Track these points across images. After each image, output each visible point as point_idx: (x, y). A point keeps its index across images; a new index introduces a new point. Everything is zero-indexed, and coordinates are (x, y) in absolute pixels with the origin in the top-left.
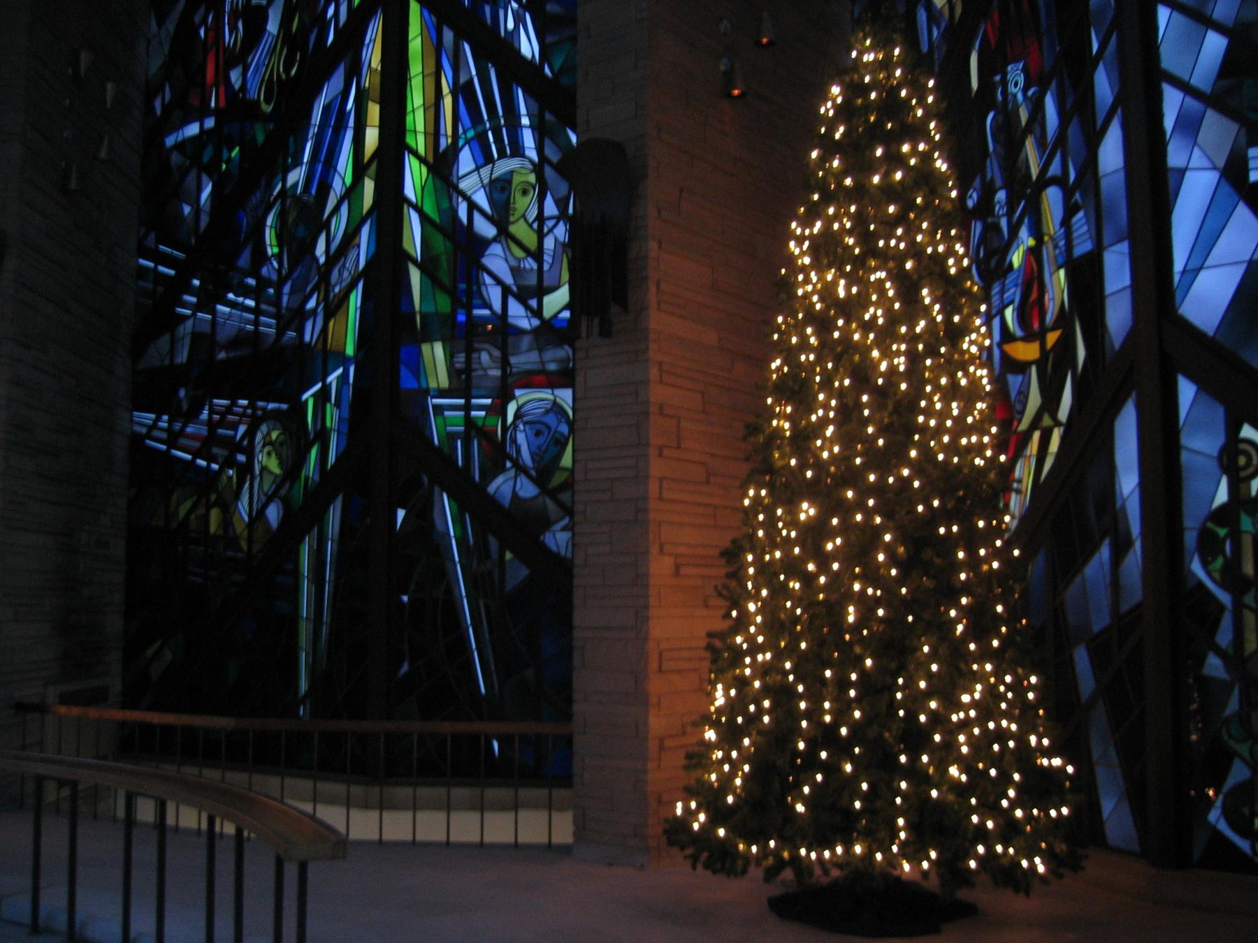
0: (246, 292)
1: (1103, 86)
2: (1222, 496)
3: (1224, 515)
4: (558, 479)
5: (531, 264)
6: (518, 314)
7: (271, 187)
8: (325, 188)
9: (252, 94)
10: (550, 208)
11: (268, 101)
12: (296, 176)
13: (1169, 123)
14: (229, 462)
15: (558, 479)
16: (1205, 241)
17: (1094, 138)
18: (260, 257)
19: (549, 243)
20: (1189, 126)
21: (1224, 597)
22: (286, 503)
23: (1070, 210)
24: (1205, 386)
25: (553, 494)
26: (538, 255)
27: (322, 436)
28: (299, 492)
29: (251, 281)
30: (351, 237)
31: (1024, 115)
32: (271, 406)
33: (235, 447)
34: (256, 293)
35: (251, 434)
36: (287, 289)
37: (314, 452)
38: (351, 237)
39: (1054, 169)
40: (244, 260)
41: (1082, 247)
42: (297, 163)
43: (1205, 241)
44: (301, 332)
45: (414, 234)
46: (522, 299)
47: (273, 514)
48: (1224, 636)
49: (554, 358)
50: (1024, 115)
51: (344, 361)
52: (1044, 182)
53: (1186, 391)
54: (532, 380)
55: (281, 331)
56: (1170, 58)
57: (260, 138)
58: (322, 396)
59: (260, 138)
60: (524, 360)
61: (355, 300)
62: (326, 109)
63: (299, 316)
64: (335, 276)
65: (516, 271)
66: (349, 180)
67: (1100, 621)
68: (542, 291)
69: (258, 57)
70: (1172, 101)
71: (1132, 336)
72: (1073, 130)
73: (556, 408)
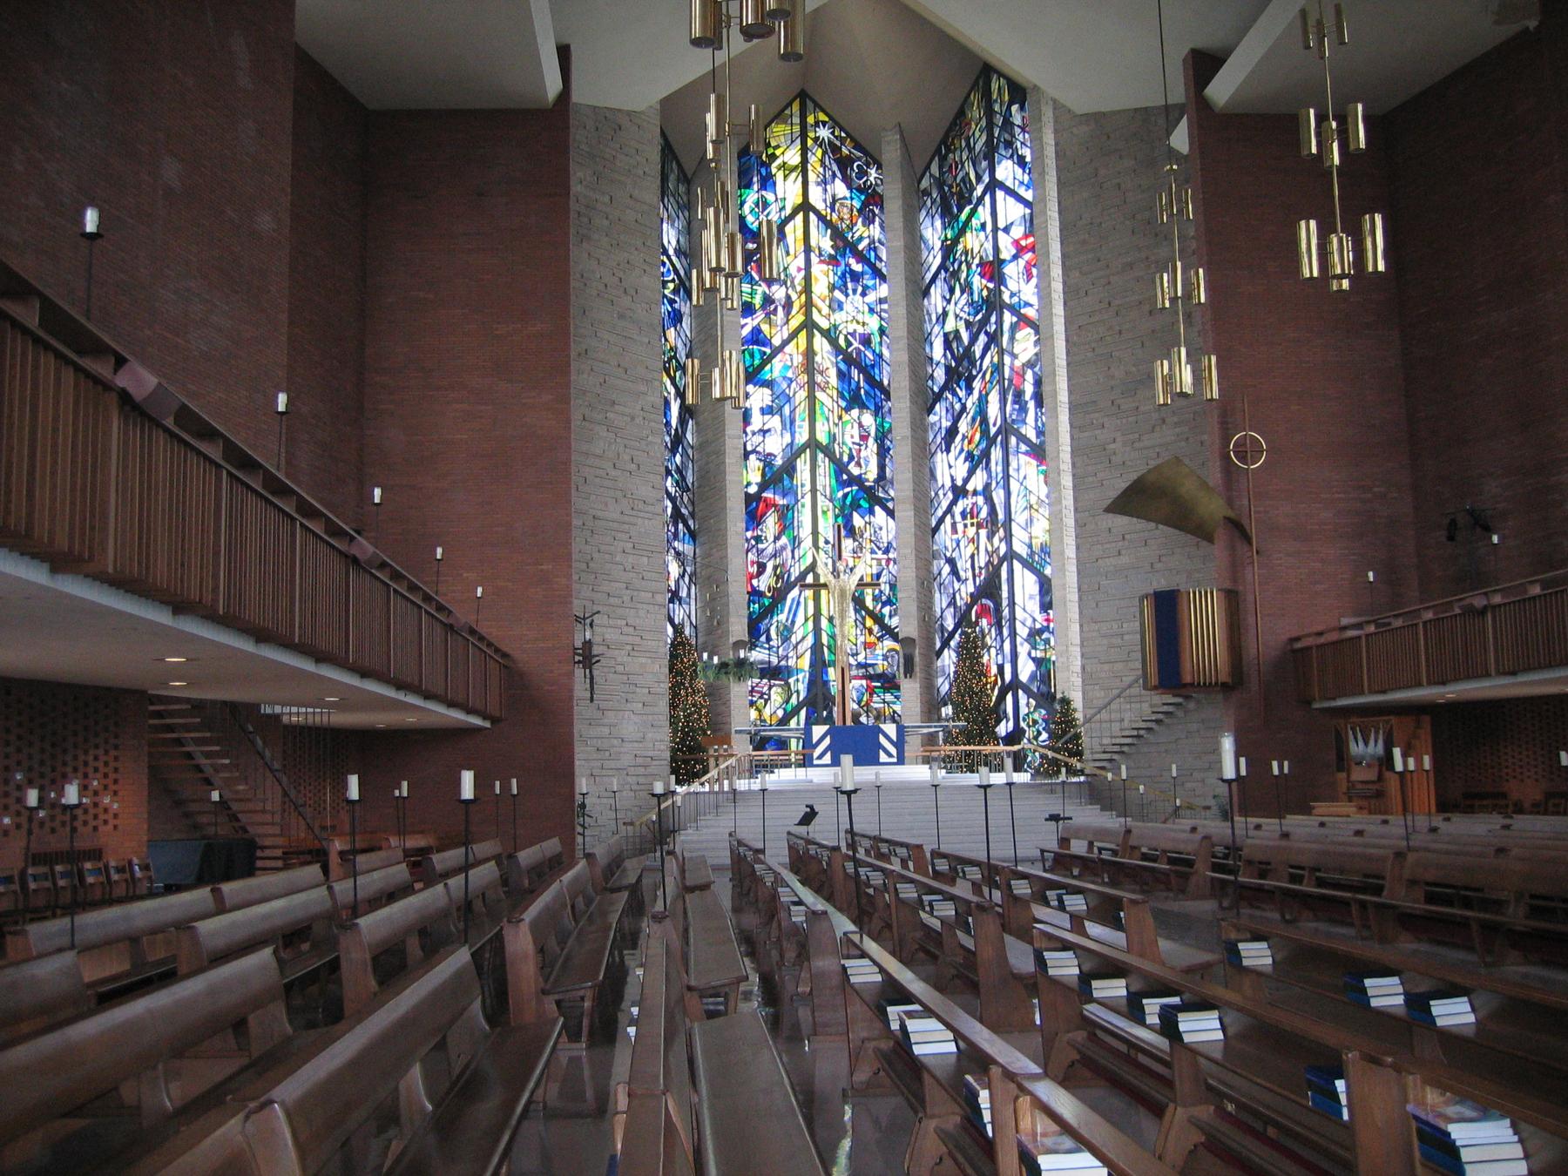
0: (765, 648)
1: (1006, 632)
2: (1026, 711)
3: (1027, 715)
4: (863, 704)
5: (854, 647)
6: (852, 661)
7: (772, 617)
8: (793, 622)
9: (763, 587)
10: (859, 632)
11: (769, 591)
12: (782, 617)
13: (1018, 643)
14: (761, 697)
15: (863, 704)
16: (1024, 666)
17: (1003, 641)
18: (769, 639)
19: (859, 642)
20: (1022, 644)
21: (1027, 728)
22: (784, 709)
23: (997, 654)
24: (1024, 691)
25: (862, 707)
26: (856, 645)
27: (798, 692)
28: (789, 708)
29: (767, 646)
30: (803, 638)
31: (987, 631)
32: (777, 682)
33: (762, 694)
34: (769, 649)
35: (770, 689)
36: (781, 649)
37: (795, 696)
38: (803, 638)
39: (994, 644)
40: (763, 638)
41: (1000, 662)
42: (782, 612)
43: (1024, 666)
44: (787, 661)
45: (825, 640)
46: (853, 655)
47: (780, 713)
48: (1027, 735)
49: (861, 672)
50: (987, 631)
51: (803, 670)
52: (991, 647)
53: (1020, 692)
54: (856, 678)
55: (779, 662)
56: (1018, 631)
57: (767, 604)
58: (798, 680)
59: (767, 604)
60: (854, 673)
61: (808, 654)
62: (793, 600)
63: (787, 657)
64: (799, 647)
65: (851, 649)
66: (803, 621)
67: (1003, 734)
68: (857, 654)
69: (763, 578)
70: (1019, 640)
71: (1011, 682)
72: (998, 638)
73: (862, 686)
